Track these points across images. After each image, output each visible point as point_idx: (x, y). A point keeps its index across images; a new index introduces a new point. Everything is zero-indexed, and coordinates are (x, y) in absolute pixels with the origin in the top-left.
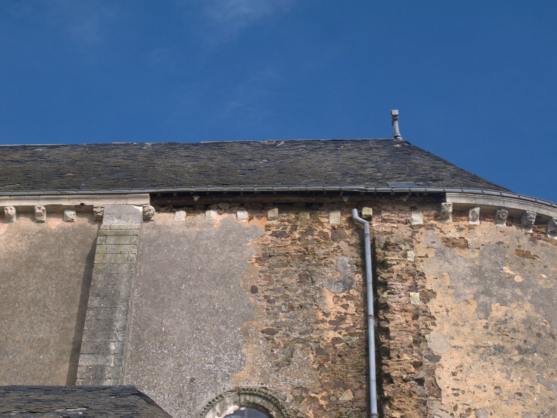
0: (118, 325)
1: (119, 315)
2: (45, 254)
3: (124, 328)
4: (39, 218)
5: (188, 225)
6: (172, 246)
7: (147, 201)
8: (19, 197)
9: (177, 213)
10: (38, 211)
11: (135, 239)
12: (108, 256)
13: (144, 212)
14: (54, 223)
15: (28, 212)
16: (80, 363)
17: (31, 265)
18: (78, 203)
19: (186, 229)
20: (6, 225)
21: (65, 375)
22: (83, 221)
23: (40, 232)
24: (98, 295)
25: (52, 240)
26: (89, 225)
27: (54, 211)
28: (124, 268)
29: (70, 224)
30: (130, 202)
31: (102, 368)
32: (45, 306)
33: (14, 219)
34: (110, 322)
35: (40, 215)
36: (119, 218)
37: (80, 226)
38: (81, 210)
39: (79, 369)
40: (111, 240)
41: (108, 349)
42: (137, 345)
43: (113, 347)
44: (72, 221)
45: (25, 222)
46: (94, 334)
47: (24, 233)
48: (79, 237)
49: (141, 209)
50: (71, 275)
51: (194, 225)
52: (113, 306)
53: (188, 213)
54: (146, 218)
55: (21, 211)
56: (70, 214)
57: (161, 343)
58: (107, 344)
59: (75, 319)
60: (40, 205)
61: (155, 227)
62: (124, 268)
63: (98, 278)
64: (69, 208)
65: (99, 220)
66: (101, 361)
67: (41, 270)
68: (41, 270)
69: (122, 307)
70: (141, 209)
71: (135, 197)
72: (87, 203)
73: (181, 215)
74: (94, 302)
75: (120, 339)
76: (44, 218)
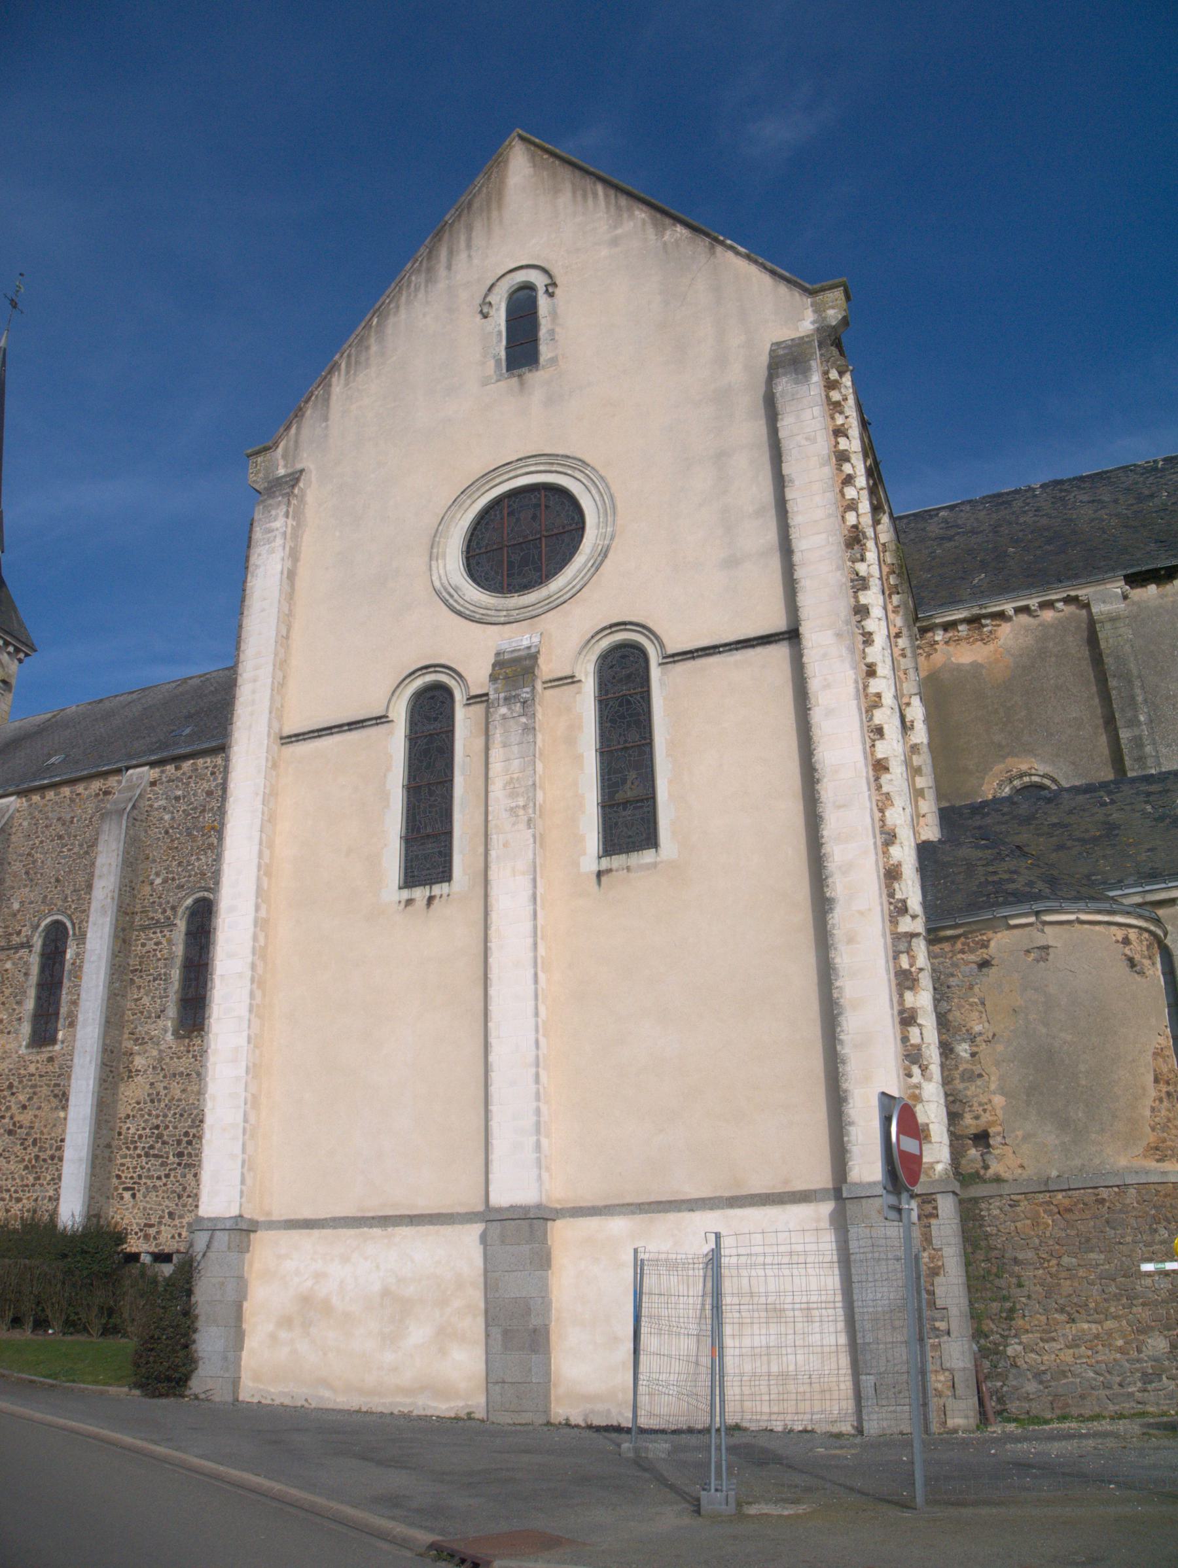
0: (1140, 699)
1: (1138, 691)
2: (1051, 644)
3: (1145, 701)
4: (1035, 614)
5: (1162, 596)
6: (1154, 618)
7: (1123, 583)
8: (1014, 600)
9: (1149, 587)
10: (1033, 608)
11: (1127, 621)
12: (1111, 641)
13: (1123, 593)
14: (1048, 615)
15: (1025, 610)
16: (1121, 736)
17: (1043, 656)
18: (1065, 595)
19: (1161, 601)
20: (1009, 624)
21: (1106, 744)
22: (1071, 609)
23: (1040, 625)
24: (1115, 676)
25: (1052, 631)
26: (1078, 611)
27: (1048, 605)
28: (1127, 648)
29: (1061, 614)
30: (1108, 586)
31: (1140, 738)
32: (1068, 690)
33: (1014, 618)
34: (1133, 698)
35: (1035, 611)
36: (1104, 602)
37: (1071, 613)
38: (1068, 600)
39: (1122, 741)
40: (1108, 626)
41: (1139, 721)
42: (1154, 710)
43: (1142, 718)
44: (1063, 610)
45: (1023, 619)
46: (1123, 710)
47: (1027, 629)
48: (1074, 624)
49: (1119, 590)
50: (1079, 659)
51: (1166, 596)
52: (1130, 682)
53: (1158, 585)
54: (1125, 597)
55: (1018, 610)
56: (1060, 605)
57: (1174, 705)
58: (1136, 717)
59: (1096, 696)
60: (1033, 603)
61: (1134, 603)
62: (1127, 648)
63: (1109, 661)
64: (1058, 600)
65: (1087, 606)
66: (1137, 732)
67: (1053, 659)
68: (1053, 659)
69: (1138, 683)
70: (1119, 590)
71: (1113, 582)
72: (1073, 593)
73: (1152, 589)
74: (1113, 683)
75: (1146, 710)
76: (1039, 613)
